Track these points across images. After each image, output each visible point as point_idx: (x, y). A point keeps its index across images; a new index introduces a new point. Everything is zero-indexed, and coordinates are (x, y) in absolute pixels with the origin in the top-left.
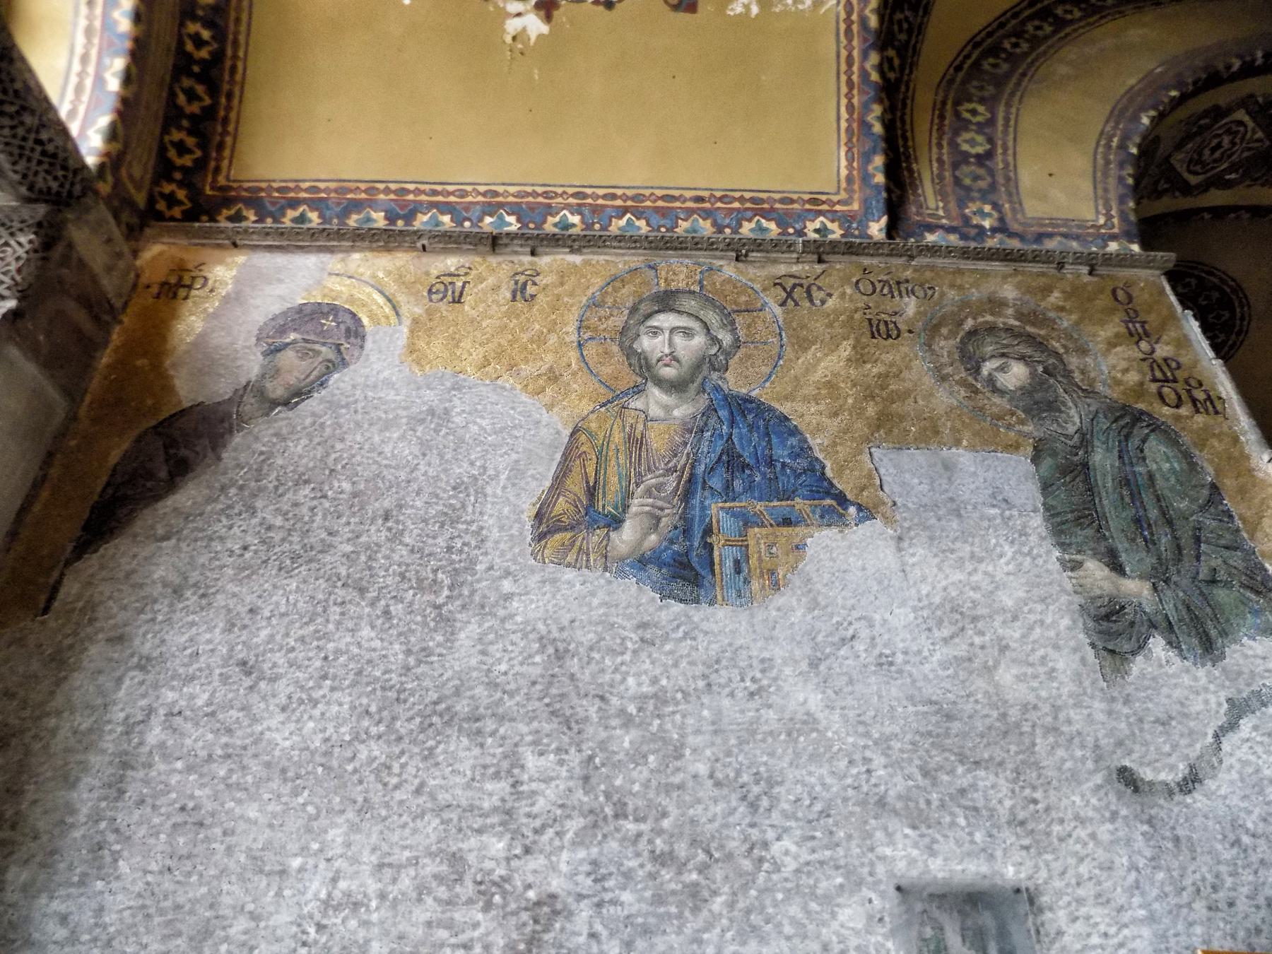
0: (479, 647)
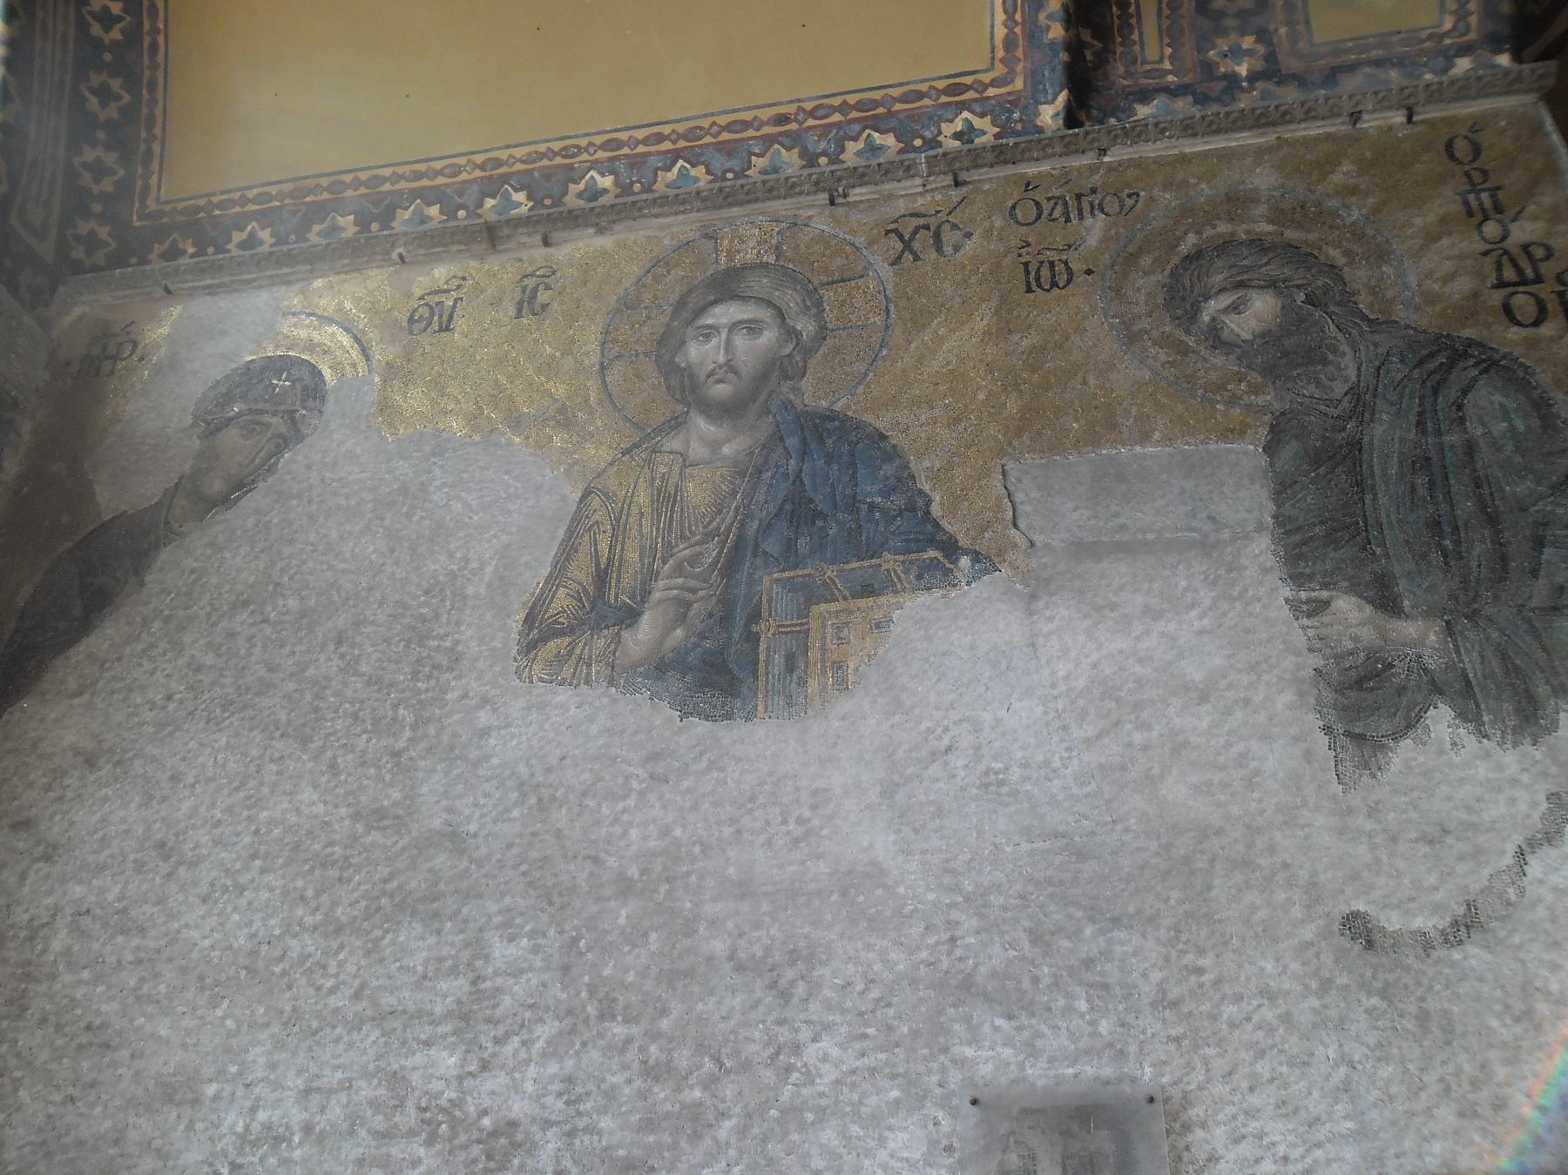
0: (444, 803)
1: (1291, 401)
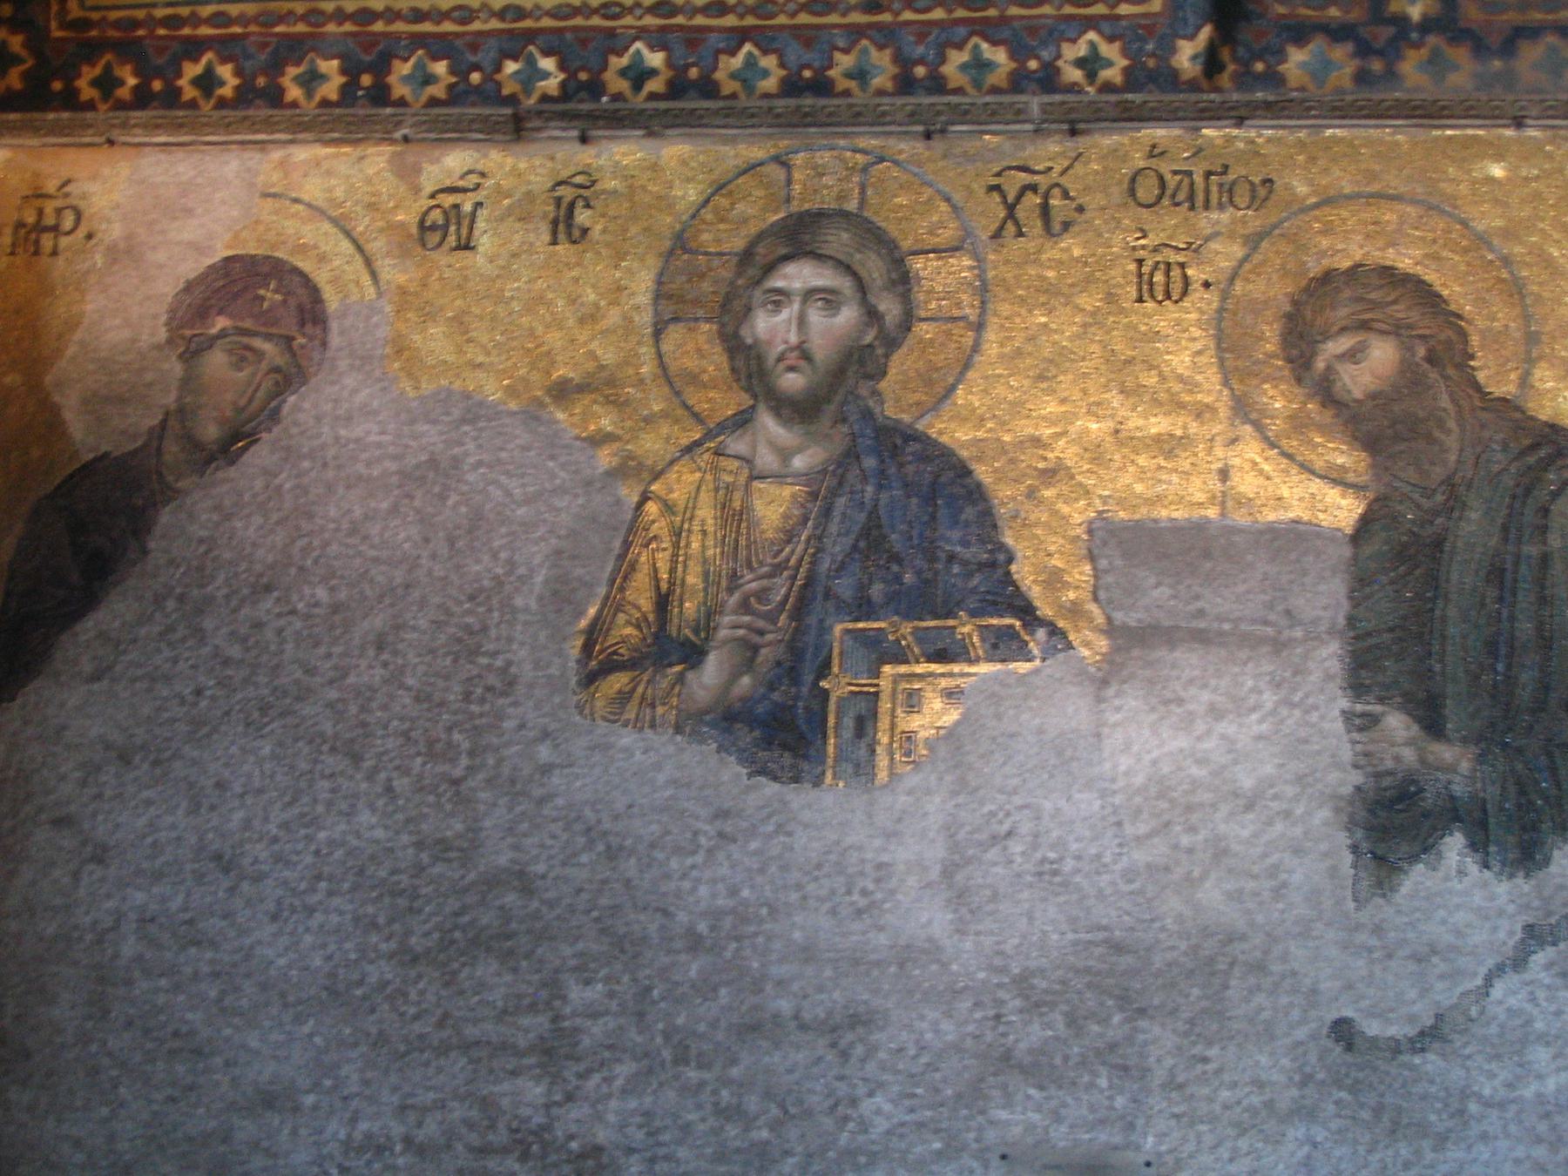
0: (510, 840)
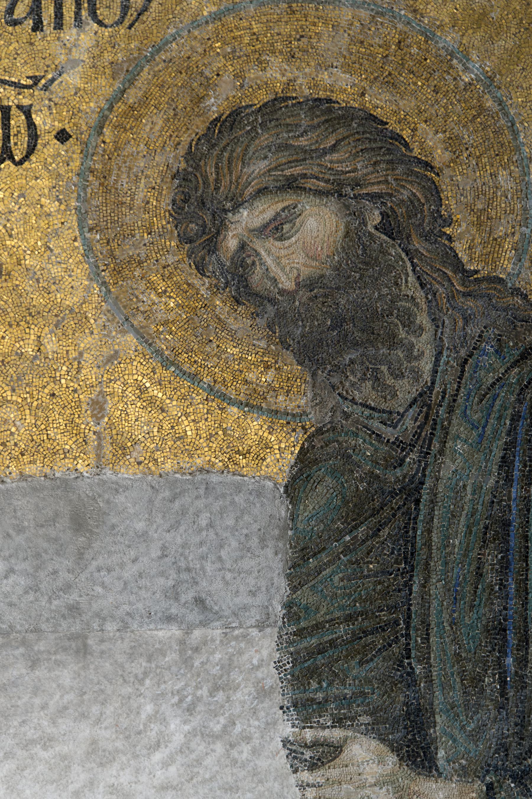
1: (333, 410)
